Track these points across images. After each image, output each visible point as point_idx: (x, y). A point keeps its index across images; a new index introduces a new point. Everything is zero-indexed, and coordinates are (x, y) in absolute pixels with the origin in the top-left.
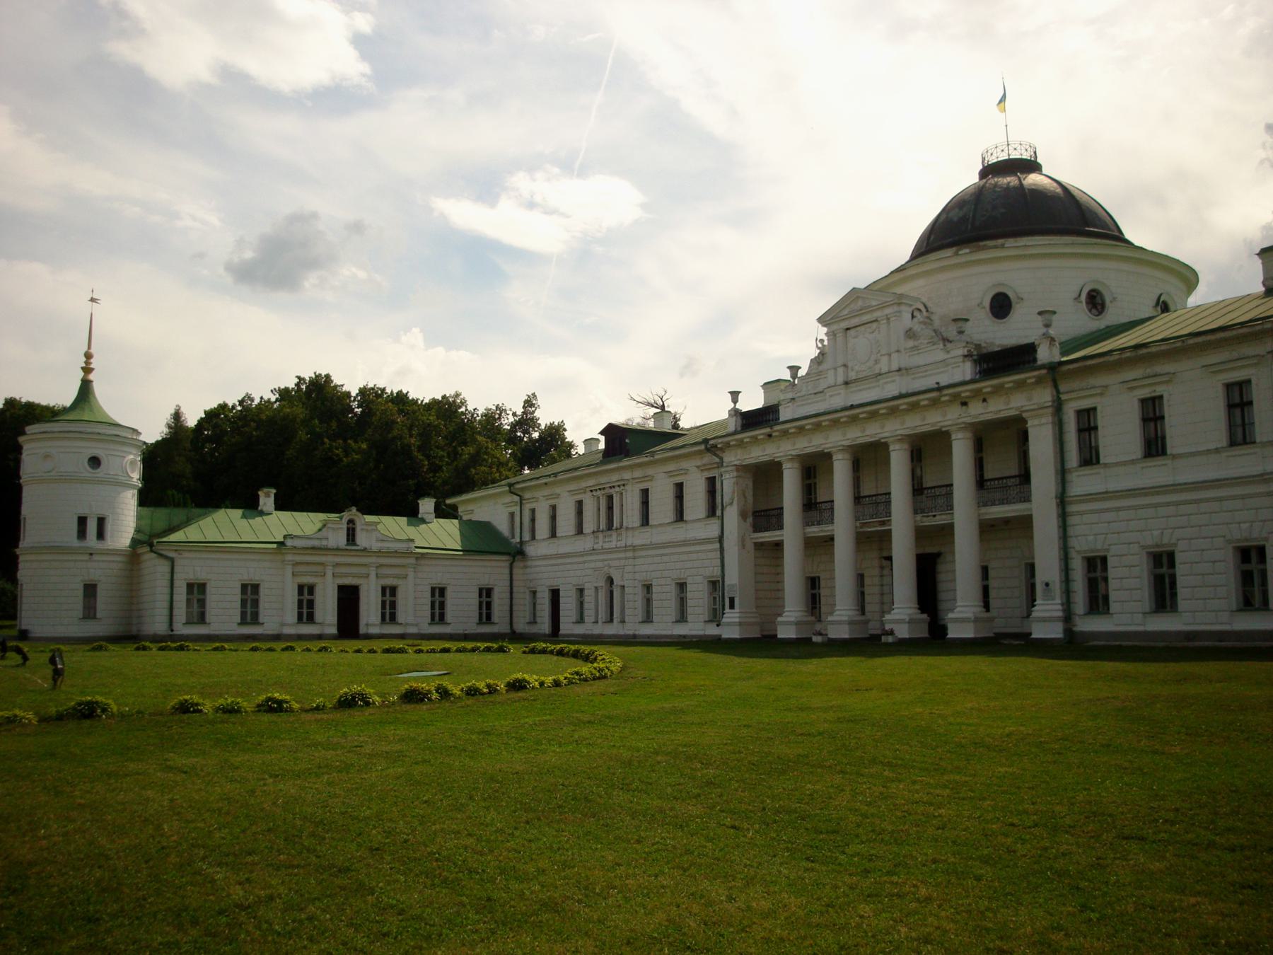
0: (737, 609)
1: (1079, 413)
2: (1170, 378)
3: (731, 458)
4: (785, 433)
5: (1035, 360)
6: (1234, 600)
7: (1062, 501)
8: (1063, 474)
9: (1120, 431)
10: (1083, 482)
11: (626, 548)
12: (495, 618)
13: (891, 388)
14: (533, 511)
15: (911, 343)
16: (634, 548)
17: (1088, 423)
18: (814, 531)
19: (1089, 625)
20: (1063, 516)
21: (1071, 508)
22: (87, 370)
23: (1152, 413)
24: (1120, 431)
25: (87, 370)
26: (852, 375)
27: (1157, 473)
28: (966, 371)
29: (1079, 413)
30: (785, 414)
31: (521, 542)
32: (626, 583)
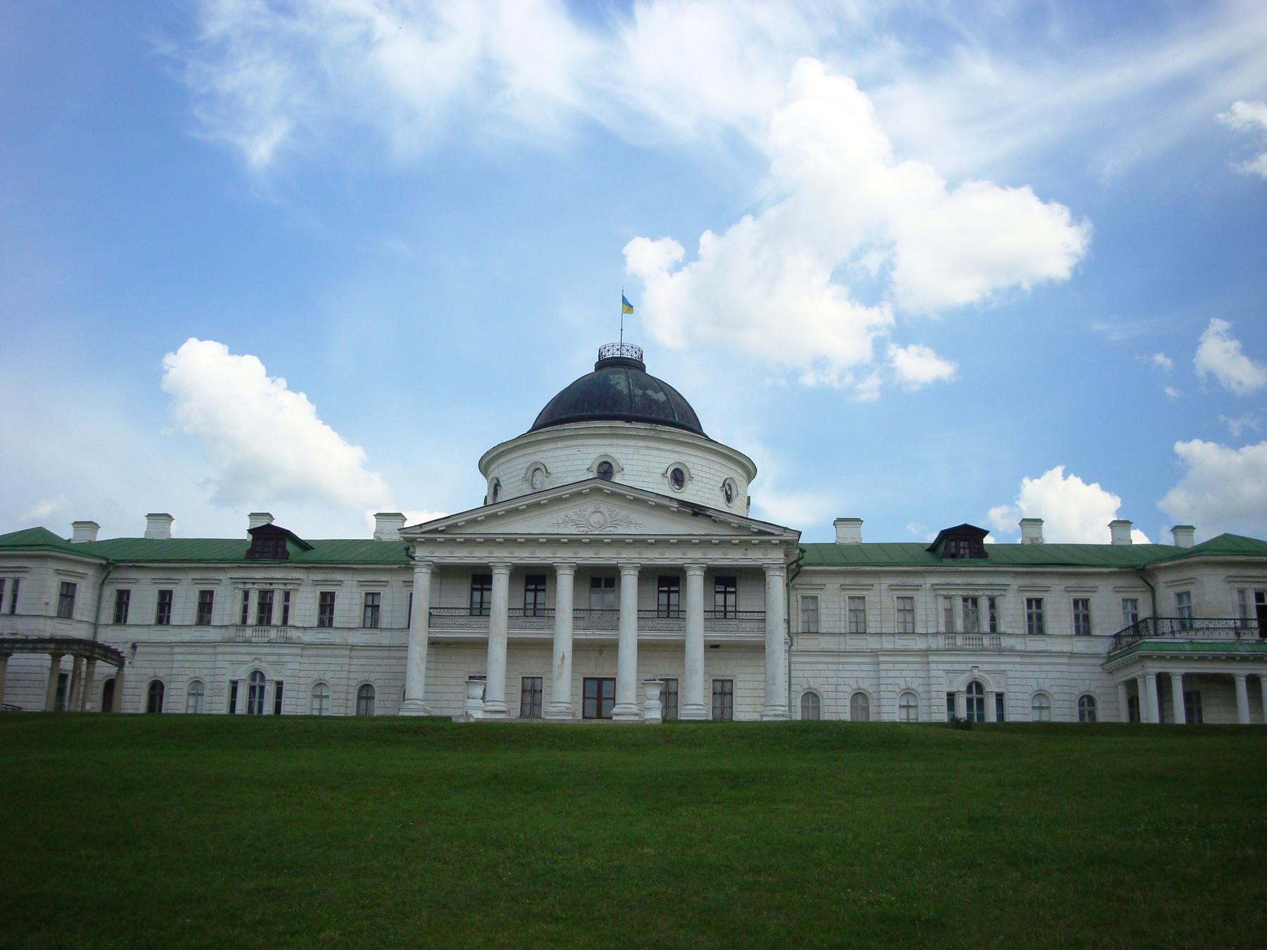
10: (803, 643)
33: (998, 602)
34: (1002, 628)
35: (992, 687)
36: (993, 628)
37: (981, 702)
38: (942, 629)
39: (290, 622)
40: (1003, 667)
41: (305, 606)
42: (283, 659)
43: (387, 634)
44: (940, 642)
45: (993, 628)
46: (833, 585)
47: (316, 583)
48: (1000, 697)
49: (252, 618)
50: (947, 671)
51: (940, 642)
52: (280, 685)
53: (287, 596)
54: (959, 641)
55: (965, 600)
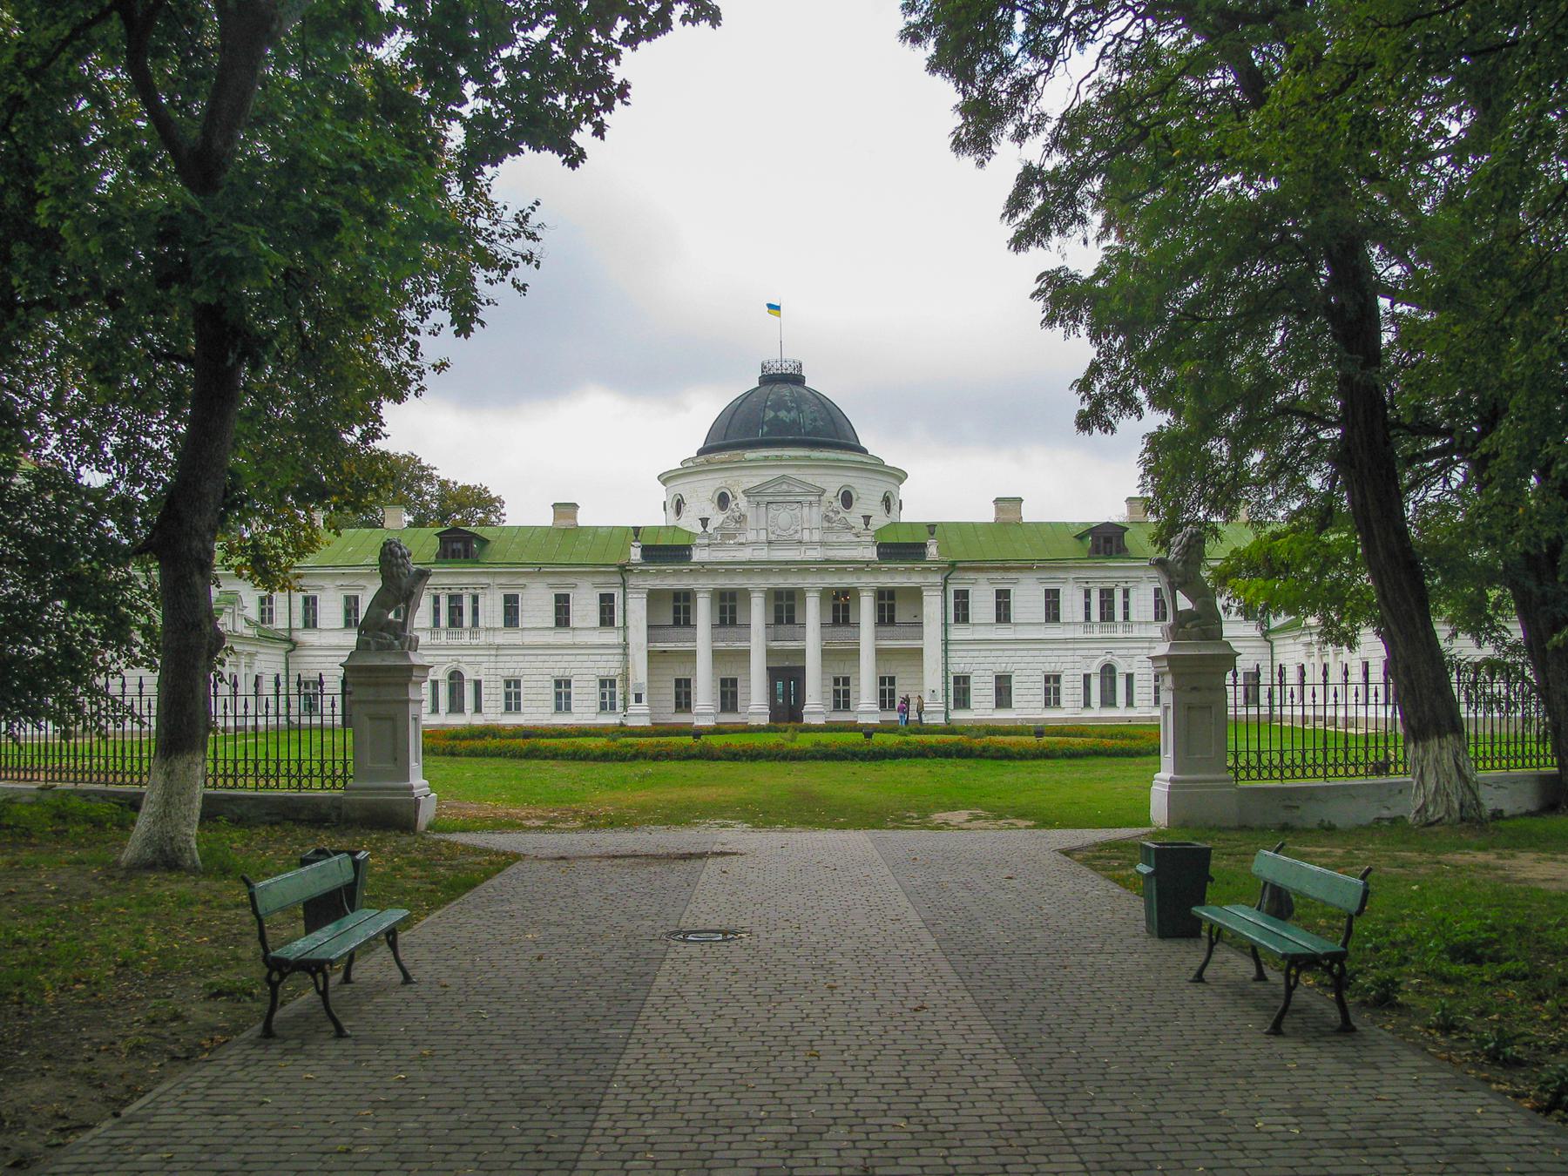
1: (957, 592)
2: (1016, 582)
5: (924, 554)
7: (946, 642)
8: (945, 625)
9: (982, 603)
10: (957, 633)
11: (489, 647)
14: (310, 604)
15: (826, 525)
16: (498, 647)
17: (962, 596)
19: (959, 715)
20: (946, 651)
23: (1003, 598)
24: (982, 603)
26: (773, 537)
27: (1004, 632)
28: (871, 553)
29: (957, 592)
30: (698, 555)
31: (290, 630)
32: (483, 678)
33: (1132, 594)
34: (1132, 617)
35: (1122, 668)
36: (1126, 617)
37: (1113, 680)
38: (1082, 619)
39: (481, 623)
40: (1132, 652)
41: (492, 608)
42: (479, 659)
44: (1079, 633)
45: (1126, 617)
46: (982, 577)
47: (502, 587)
48: (1129, 677)
49: (444, 621)
50: (1085, 657)
51: (1079, 633)
52: (478, 684)
53: (475, 599)
54: (1097, 629)
55: (1102, 591)
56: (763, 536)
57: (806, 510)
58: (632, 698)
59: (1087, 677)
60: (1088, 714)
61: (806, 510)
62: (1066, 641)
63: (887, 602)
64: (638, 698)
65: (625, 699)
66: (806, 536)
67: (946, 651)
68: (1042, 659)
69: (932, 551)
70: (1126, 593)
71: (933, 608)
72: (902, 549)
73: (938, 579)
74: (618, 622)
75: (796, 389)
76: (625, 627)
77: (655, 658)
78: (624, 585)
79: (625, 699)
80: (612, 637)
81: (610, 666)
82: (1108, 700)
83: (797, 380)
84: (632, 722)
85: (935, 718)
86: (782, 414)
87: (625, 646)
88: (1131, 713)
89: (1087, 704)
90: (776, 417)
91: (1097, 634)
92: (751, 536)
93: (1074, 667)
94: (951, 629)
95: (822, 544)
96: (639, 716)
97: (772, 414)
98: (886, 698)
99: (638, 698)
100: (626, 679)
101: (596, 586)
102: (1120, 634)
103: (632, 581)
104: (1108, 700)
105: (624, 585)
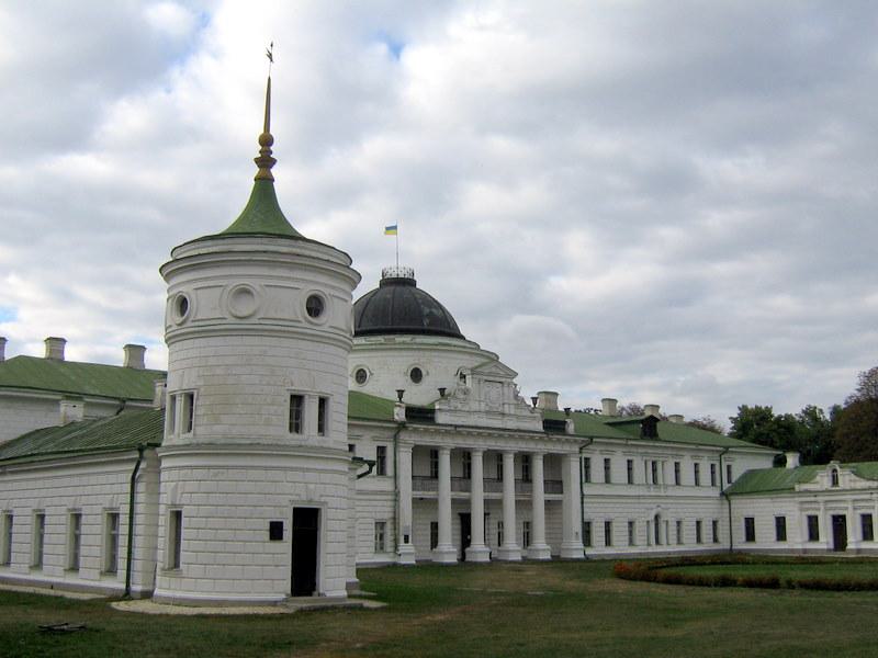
0: (410, 544)
3: (410, 439)
4: (437, 432)
6: (806, 537)
7: (583, 496)
12: (720, 536)
13: (511, 424)
15: (515, 402)
18: (464, 495)
19: (589, 551)
20: (582, 503)
21: (585, 500)
22: (266, 161)
25: (266, 161)
28: (539, 426)
30: (441, 418)
43: (598, 486)
50: (648, 509)
56: (483, 407)
57: (506, 389)
58: (402, 538)
59: (648, 522)
60: (650, 550)
61: (506, 389)
62: (639, 497)
63: (553, 461)
64: (406, 540)
65: (396, 541)
66: (507, 411)
67: (582, 503)
68: (370, 509)
69: (571, 428)
70: (663, 462)
71: (573, 470)
72: (554, 425)
73: (577, 450)
74: (389, 470)
75: (406, 289)
76: (395, 476)
77: (418, 503)
78: (395, 438)
79: (396, 541)
80: (387, 485)
81: (385, 513)
82: (657, 542)
83: (408, 282)
84: (404, 561)
85: (580, 555)
86: (434, 310)
87: (396, 494)
88: (669, 549)
89: (649, 545)
90: (431, 312)
91: (653, 494)
92: (474, 406)
93: (643, 516)
94: (584, 485)
95: (517, 417)
96: (408, 555)
97: (427, 311)
98: (550, 538)
99: (406, 540)
100: (395, 519)
101: (375, 439)
102: (662, 494)
103: (404, 436)
104: (657, 542)
105: (395, 438)
